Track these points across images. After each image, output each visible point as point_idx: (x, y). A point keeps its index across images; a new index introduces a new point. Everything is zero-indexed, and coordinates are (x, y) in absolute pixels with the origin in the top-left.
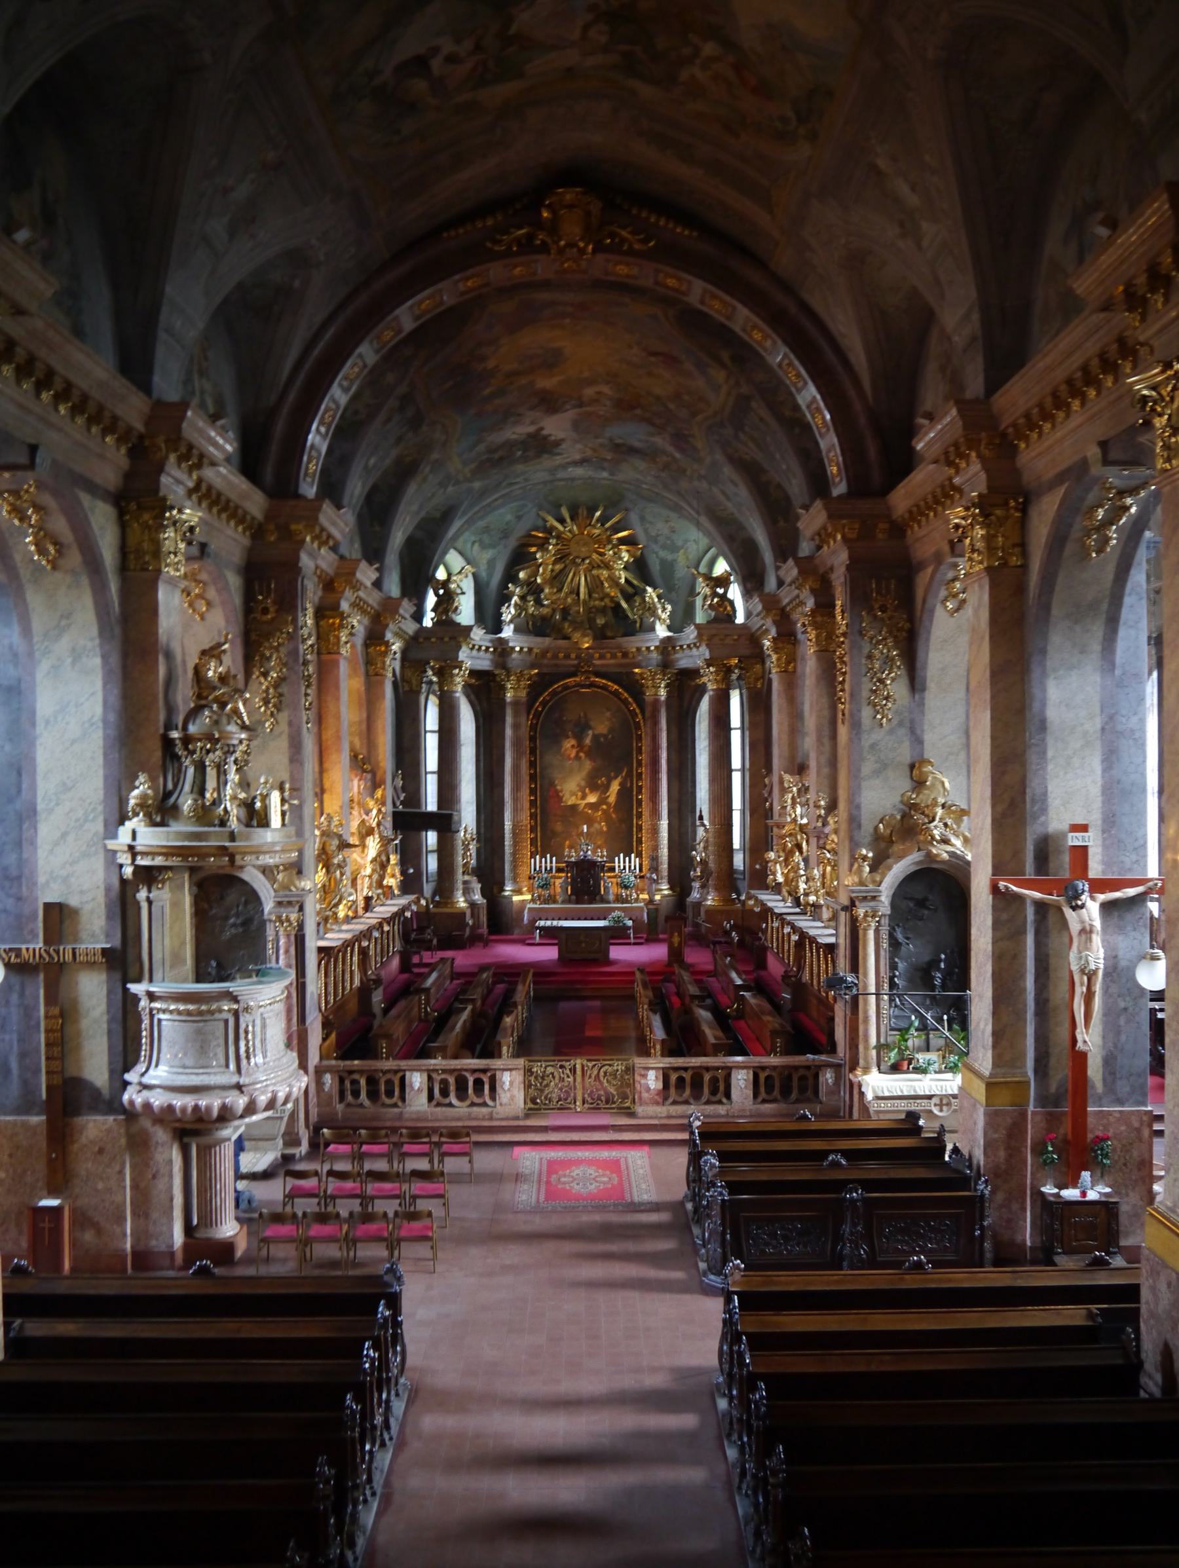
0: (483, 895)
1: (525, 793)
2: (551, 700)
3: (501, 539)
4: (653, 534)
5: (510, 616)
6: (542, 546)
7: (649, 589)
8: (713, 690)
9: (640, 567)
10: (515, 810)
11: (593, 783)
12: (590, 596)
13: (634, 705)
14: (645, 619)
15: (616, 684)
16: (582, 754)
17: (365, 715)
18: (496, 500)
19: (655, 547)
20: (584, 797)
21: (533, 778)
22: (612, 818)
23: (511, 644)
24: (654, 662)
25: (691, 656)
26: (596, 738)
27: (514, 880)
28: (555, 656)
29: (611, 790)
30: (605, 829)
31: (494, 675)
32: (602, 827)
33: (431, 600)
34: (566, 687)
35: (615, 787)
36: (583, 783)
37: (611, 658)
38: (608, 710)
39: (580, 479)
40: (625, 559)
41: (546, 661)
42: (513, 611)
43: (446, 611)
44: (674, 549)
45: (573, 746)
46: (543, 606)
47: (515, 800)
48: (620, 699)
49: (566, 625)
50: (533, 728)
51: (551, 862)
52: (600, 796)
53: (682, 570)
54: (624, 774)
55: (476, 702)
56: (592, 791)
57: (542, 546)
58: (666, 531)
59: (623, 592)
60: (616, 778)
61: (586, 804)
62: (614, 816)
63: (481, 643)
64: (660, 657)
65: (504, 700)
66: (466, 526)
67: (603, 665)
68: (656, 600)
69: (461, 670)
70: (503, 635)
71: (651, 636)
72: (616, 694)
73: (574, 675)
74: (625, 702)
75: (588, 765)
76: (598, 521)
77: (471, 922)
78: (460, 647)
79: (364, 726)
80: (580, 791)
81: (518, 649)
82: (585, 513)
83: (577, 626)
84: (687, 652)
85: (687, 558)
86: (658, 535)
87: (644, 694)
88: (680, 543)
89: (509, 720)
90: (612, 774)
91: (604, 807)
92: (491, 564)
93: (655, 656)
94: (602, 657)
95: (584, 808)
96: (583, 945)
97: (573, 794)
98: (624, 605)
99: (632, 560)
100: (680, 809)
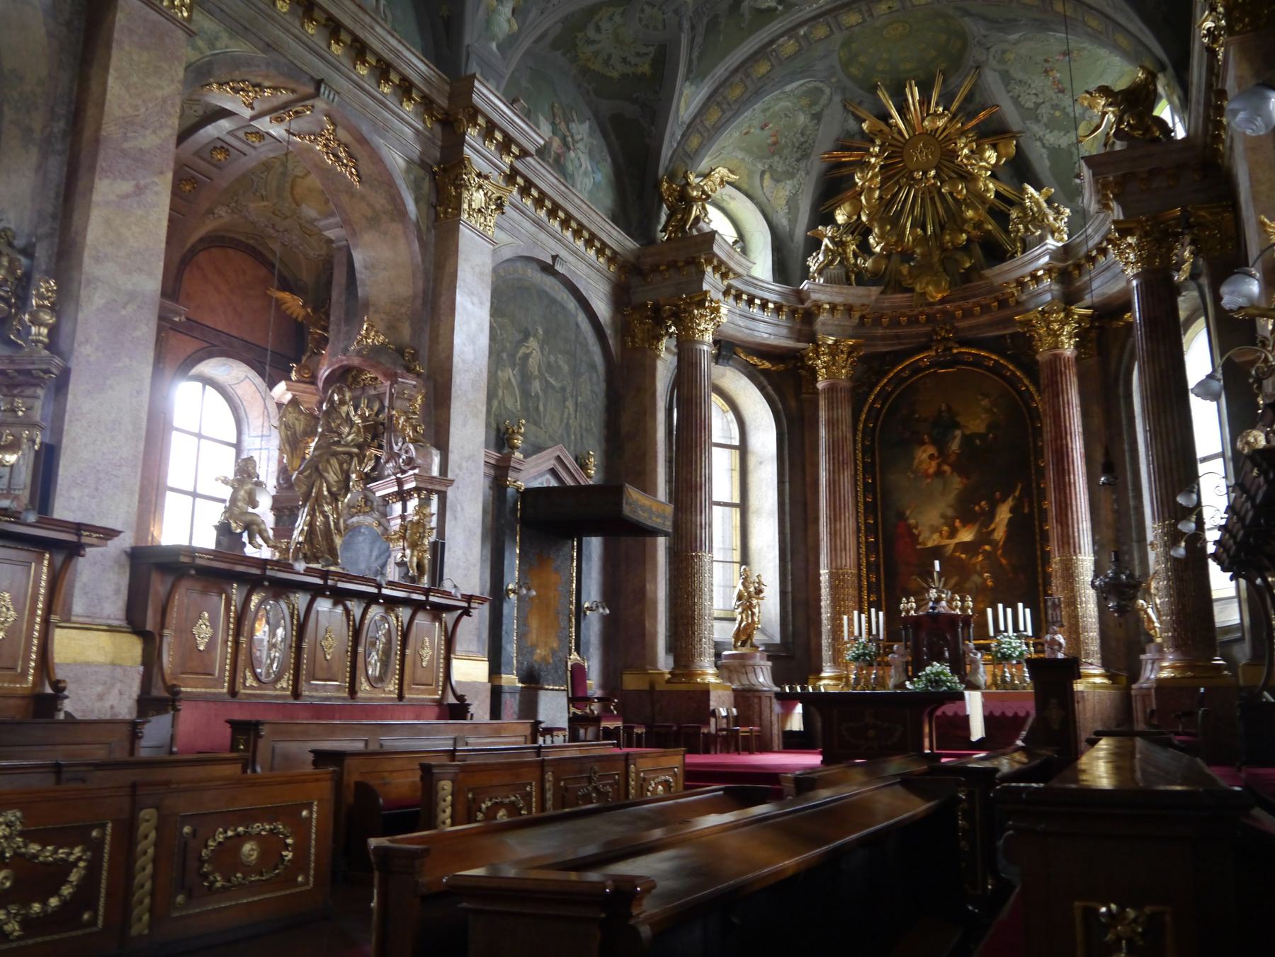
1: (849, 524)
2: (892, 392)
3: (798, 160)
4: (1030, 105)
6: (865, 166)
7: (1031, 190)
8: (1135, 276)
10: (833, 550)
11: (965, 512)
12: (942, 227)
13: (1026, 381)
16: (946, 468)
18: (754, 57)
19: (1037, 129)
20: (953, 533)
21: (870, 509)
22: (1001, 565)
23: (814, 296)
25: (1108, 268)
26: (968, 440)
27: (836, 661)
28: (895, 323)
29: (997, 520)
30: (990, 583)
32: (985, 580)
34: (916, 369)
35: (1004, 514)
36: (950, 512)
37: (982, 312)
40: (993, 161)
41: (880, 331)
42: (821, 257)
45: (931, 457)
47: (833, 534)
48: (1003, 377)
49: (905, 269)
52: (979, 533)
54: (1017, 494)
55: (776, 397)
56: (965, 523)
58: (1051, 93)
60: (1003, 500)
61: (957, 544)
62: (1004, 561)
63: (767, 295)
64: (1056, 287)
65: (815, 392)
66: (714, 115)
67: (971, 328)
68: (1045, 205)
71: (1038, 251)
72: (997, 370)
74: (1013, 382)
75: (957, 483)
76: (937, 104)
78: (702, 273)
79: (419, 301)
80: (946, 524)
81: (827, 306)
86: (1038, 105)
87: (1036, 352)
90: (998, 494)
91: (987, 548)
92: (792, 203)
94: (968, 314)
95: (955, 550)
96: (871, 733)
97: (935, 529)
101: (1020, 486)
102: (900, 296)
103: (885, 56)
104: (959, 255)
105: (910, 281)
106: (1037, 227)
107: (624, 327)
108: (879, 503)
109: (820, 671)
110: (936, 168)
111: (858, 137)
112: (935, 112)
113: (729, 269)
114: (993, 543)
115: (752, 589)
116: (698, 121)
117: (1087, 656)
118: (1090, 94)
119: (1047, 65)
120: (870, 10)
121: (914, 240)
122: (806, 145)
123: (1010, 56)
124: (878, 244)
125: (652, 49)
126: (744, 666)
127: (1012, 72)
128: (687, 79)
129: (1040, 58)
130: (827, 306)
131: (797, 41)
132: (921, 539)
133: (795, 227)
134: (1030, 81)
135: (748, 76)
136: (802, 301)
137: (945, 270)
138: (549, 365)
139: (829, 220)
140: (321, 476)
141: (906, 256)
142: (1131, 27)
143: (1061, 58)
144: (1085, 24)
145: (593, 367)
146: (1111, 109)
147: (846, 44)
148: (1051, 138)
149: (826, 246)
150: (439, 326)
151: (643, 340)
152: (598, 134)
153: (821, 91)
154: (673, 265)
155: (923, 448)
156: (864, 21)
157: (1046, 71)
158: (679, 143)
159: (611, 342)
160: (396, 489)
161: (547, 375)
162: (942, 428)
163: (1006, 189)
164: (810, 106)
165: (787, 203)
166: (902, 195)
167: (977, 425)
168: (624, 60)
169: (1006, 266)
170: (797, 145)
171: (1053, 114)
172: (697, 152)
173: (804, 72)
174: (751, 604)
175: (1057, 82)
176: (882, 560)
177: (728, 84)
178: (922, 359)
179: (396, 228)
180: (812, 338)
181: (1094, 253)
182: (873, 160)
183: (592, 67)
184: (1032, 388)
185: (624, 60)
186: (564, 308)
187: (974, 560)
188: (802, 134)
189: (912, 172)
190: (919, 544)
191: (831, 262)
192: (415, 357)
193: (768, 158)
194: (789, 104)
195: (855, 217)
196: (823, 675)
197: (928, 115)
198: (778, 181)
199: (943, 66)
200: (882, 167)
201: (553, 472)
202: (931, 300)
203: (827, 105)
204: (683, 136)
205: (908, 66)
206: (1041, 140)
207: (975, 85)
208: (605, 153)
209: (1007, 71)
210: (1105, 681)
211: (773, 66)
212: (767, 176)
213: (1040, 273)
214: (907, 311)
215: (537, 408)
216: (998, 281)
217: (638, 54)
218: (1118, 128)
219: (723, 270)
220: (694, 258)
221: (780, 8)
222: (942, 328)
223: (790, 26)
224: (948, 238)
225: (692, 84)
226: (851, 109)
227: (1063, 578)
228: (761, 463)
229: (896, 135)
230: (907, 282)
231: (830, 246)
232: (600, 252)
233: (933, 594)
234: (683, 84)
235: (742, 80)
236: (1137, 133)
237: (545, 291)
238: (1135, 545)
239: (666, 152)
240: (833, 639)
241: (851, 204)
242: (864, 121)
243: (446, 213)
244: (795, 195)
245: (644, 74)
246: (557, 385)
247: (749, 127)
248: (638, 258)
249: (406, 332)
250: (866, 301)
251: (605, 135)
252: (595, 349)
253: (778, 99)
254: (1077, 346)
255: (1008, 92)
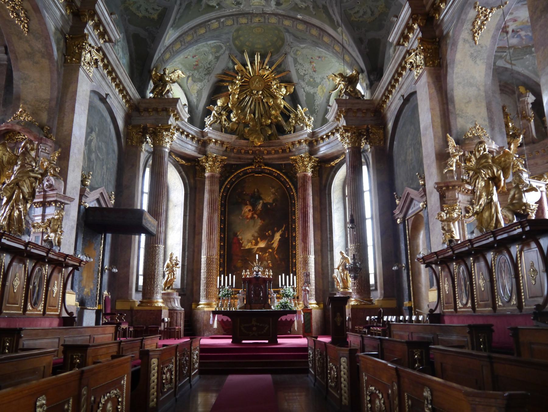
0: (182, 305)
1: (216, 236)
2: (235, 181)
3: (205, 75)
4: (302, 74)
5: (210, 122)
6: (233, 83)
7: (300, 107)
8: (348, 148)
9: (294, 99)
10: (209, 248)
11: (262, 235)
12: (262, 116)
13: (290, 184)
14: (297, 127)
15: (278, 170)
16: (255, 216)
17: (55, 94)
18: (200, 25)
20: (257, 243)
21: (222, 231)
23: (209, 135)
24: (303, 151)
26: (265, 205)
27: (207, 296)
28: (239, 152)
29: (275, 239)
30: (270, 265)
31: (198, 161)
32: (268, 264)
33: (151, 85)
34: (245, 173)
35: (277, 237)
36: (256, 235)
37: (275, 153)
38: (273, 187)
39: (257, 15)
40: (284, 93)
41: (233, 155)
43: (161, 93)
44: (315, 85)
45: (250, 210)
46: (231, 121)
47: (209, 240)
49: (246, 130)
50: (224, 198)
51: (232, 279)
52: (267, 243)
53: (320, 99)
54: (283, 229)
56: (262, 240)
57: (233, 83)
58: (310, 71)
59: (282, 113)
60: (278, 231)
62: (276, 256)
64: (307, 148)
66: (178, 46)
67: (270, 159)
68: (304, 114)
69: (169, 131)
70: (206, 130)
72: (278, 177)
73: (252, 165)
74: (284, 183)
75: (259, 222)
77: (166, 320)
78: (170, 116)
79: (54, 103)
82: (259, 57)
83: (253, 131)
84: (327, 140)
85: (323, 91)
86: (305, 75)
87: (296, 173)
88: (318, 80)
89: (207, 187)
90: (276, 228)
91: (270, 250)
92: (199, 92)
93: (305, 147)
94: (269, 153)
96: (254, 329)
97: (249, 241)
98: (284, 123)
99: (288, 93)
100: (321, 251)
101: (284, 226)
102: (243, 141)
103: (251, 39)
104: (267, 128)
105: (247, 136)
106: (301, 123)
107: (128, 135)
108: (226, 228)
109: (199, 301)
110: (262, 90)
111: (232, 71)
112: (265, 68)
113: (180, 116)
114: (273, 249)
115: (174, 263)
116: (171, 47)
117: (311, 296)
118: (335, 76)
119: (312, 60)
120: (251, 19)
121: (250, 119)
122: (210, 69)
123: (299, 53)
124: (234, 117)
125: (160, 8)
126: (170, 299)
127: (298, 59)
128: (172, 26)
129: (310, 57)
130: (214, 140)
131: (219, 24)
132: (243, 245)
133: (199, 103)
134: (304, 65)
135: (195, 32)
136: (203, 136)
137: (262, 133)
138: (99, 147)
139: (215, 104)
140: (19, 188)
141: (246, 125)
142: (354, 54)
143: (318, 58)
144: (333, 48)
145: (114, 151)
146: (343, 83)
147: (237, 30)
148: (308, 89)
149: (214, 114)
150: (64, 117)
151: (137, 142)
152: (126, 41)
153: (222, 48)
154: (156, 110)
155: (246, 206)
156: (248, 22)
157: (311, 62)
158: (162, 55)
159: (123, 140)
160: (42, 200)
161: (98, 152)
162: (255, 199)
163: (287, 105)
164: (215, 53)
165: (197, 92)
166: (247, 99)
167: (269, 199)
168: (147, 10)
169: (288, 136)
170: (206, 68)
171: (310, 80)
172: (167, 61)
173: (217, 37)
174: (173, 270)
175: (313, 67)
176: (226, 253)
177: (187, 34)
178: (248, 169)
179: (45, 62)
180: (204, 153)
181: (325, 137)
182: (237, 82)
183: (131, 8)
184: (292, 187)
185: (147, 10)
186: (106, 120)
187: (264, 255)
188: (209, 64)
189: (252, 90)
190: (242, 247)
191: (216, 122)
192: (50, 131)
193: (192, 71)
194: (207, 50)
195: (226, 104)
196: (200, 303)
197: (262, 68)
198: (195, 82)
199: (272, 50)
200: (240, 85)
201: (98, 200)
202: (256, 145)
203: (222, 54)
204: (164, 52)
205: (258, 46)
206: (303, 88)
207: (283, 61)
208: (127, 51)
209: (296, 59)
210: (317, 306)
211: (206, 31)
212: (190, 78)
213: (302, 141)
214: (245, 148)
215: (93, 167)
216: (285, 141)
217: (153, 9)
218: (346, 91)
219: (178, 117)
220: (166, 108)
221: (217, 7)
222: (258, 157)
223: (220, 16)
224: (263, 120)
225: (173, 29)
226: (232, 58)
227: (303, 264)
228: (176, 206)
229: (248, 74)
230: (246, 136)
231: (216, 115)
232: (124, 97)
233: (256, 269)
234: (169, 28)
235: (192, 34)
236: (353, 94)
237: (100, 110)
238: (329, 252)
239: (156, 57)
240: (207, 287)
241: (225, 98)
242: (236, 64)
243: (71, 60)
244: (201, 89)
245: (153, 19)
246: (101, 157)
247: (188, 55)
248: (139, 103)
249: (44, 117)
250: (230, 141)
251: (128, 42)
252: (115, 142)
253: (203, 46)
254: (312, 172)
255: (295, 67)
